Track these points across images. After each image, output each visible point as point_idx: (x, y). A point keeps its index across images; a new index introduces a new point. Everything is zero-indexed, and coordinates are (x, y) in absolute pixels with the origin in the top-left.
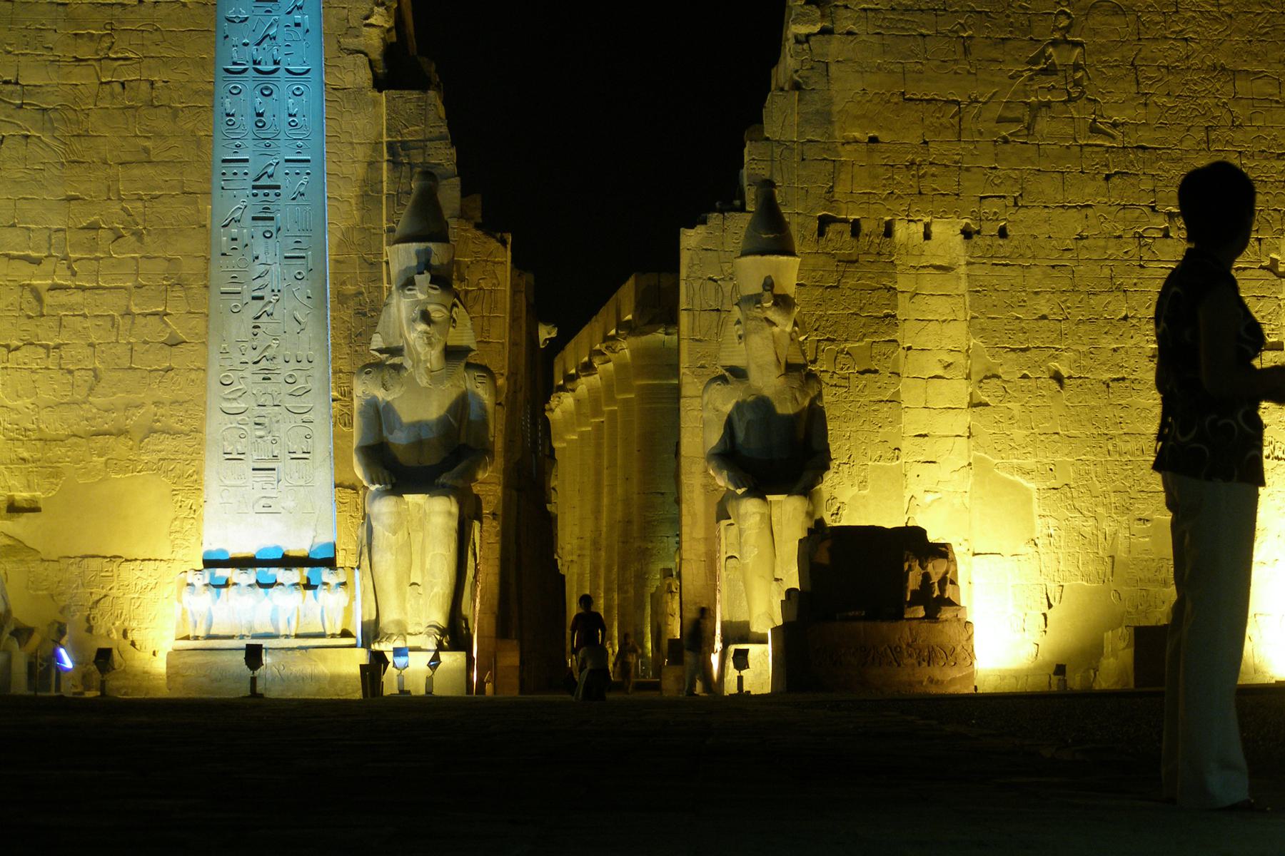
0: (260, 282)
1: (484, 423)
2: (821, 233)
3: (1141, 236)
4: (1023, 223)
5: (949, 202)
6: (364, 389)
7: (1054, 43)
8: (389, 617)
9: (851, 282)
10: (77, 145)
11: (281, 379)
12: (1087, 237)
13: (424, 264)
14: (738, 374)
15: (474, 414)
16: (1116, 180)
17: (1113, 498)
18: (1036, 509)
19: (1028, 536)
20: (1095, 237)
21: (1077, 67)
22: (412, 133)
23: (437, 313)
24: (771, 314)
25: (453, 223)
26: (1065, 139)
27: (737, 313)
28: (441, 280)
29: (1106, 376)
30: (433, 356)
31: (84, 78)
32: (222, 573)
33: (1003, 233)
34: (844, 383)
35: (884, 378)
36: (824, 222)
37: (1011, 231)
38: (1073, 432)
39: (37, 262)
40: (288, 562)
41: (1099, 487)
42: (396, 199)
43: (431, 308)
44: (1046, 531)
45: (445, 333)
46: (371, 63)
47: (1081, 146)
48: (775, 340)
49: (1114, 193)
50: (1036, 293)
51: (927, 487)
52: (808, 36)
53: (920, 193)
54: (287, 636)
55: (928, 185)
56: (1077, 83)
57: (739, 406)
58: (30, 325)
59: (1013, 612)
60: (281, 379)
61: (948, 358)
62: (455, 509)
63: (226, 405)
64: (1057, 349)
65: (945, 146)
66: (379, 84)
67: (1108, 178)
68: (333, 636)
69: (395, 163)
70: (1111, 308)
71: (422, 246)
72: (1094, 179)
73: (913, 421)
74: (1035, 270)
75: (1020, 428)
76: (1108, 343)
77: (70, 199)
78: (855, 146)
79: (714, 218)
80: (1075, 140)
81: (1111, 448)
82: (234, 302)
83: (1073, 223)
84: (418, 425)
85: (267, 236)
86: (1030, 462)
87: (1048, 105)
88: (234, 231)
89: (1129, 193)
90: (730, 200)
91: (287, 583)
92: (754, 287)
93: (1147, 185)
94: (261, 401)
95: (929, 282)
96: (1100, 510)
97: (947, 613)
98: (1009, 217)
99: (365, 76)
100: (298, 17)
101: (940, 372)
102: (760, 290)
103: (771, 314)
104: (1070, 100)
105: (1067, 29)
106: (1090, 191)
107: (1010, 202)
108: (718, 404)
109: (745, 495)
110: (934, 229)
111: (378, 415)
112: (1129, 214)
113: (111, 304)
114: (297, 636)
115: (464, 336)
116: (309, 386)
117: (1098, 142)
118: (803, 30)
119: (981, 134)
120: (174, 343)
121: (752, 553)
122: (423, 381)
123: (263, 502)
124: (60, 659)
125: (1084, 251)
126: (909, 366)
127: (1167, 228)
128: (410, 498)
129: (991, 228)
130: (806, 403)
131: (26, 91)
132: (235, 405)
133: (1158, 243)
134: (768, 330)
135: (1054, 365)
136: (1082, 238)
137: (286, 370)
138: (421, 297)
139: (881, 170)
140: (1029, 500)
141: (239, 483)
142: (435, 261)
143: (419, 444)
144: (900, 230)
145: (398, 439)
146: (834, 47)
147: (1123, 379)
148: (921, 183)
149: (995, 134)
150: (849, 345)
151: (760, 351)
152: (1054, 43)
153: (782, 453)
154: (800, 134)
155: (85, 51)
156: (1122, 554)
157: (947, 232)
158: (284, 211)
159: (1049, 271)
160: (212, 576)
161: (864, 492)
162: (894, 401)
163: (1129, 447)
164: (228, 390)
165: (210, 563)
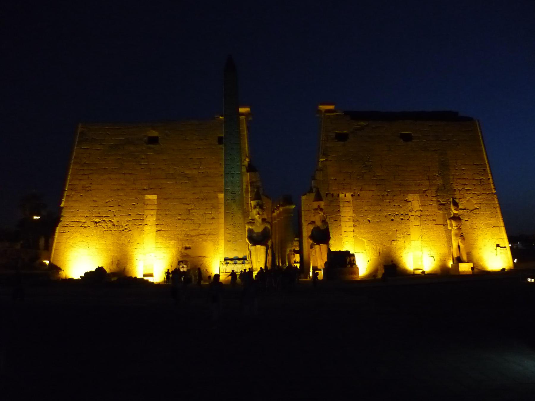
4: (363, 193)
5: (349, 190)
14: (313, 222)
17: (379, 242)
18: (366, 244)
21: (371, 165)
22: (254, 180)
23: (261, 213)
25: (262, 196)
27: (313, 211)
30: (260, 221)
31: (195, 172)
32: (227, 261)
33: (359, 195)
35: (338, 221)
36: (327, 194)
37: (361, 195)
39: (189, 204)
41: (377, 240)
42: (251, 192)
46: (246, 168)
48: (320, 217)
59: (364, 265)
66: (248, 171)
69: (250, 185)
73: (344, 229)
77: (194, 193)
79: (308, 194)
83: (371, 193)
84: (258, 233)
85: (234, 202)
86: (364, 236)
90: (311, 191)
92: (316, 207)
95: (346, 204)
97: (354, 266)
110: (347, 195)
111: (250, 231)
113: (202, 212)
120: (213, 218)
121: (318, 254)
122: (258, 225)
126: (342, 219)
131: (186, 174)
151: (317, 219)
153: (322, 236)
155: (196, 167)
156: (381, 252)
157: (349, 195)
162: (340, 225)
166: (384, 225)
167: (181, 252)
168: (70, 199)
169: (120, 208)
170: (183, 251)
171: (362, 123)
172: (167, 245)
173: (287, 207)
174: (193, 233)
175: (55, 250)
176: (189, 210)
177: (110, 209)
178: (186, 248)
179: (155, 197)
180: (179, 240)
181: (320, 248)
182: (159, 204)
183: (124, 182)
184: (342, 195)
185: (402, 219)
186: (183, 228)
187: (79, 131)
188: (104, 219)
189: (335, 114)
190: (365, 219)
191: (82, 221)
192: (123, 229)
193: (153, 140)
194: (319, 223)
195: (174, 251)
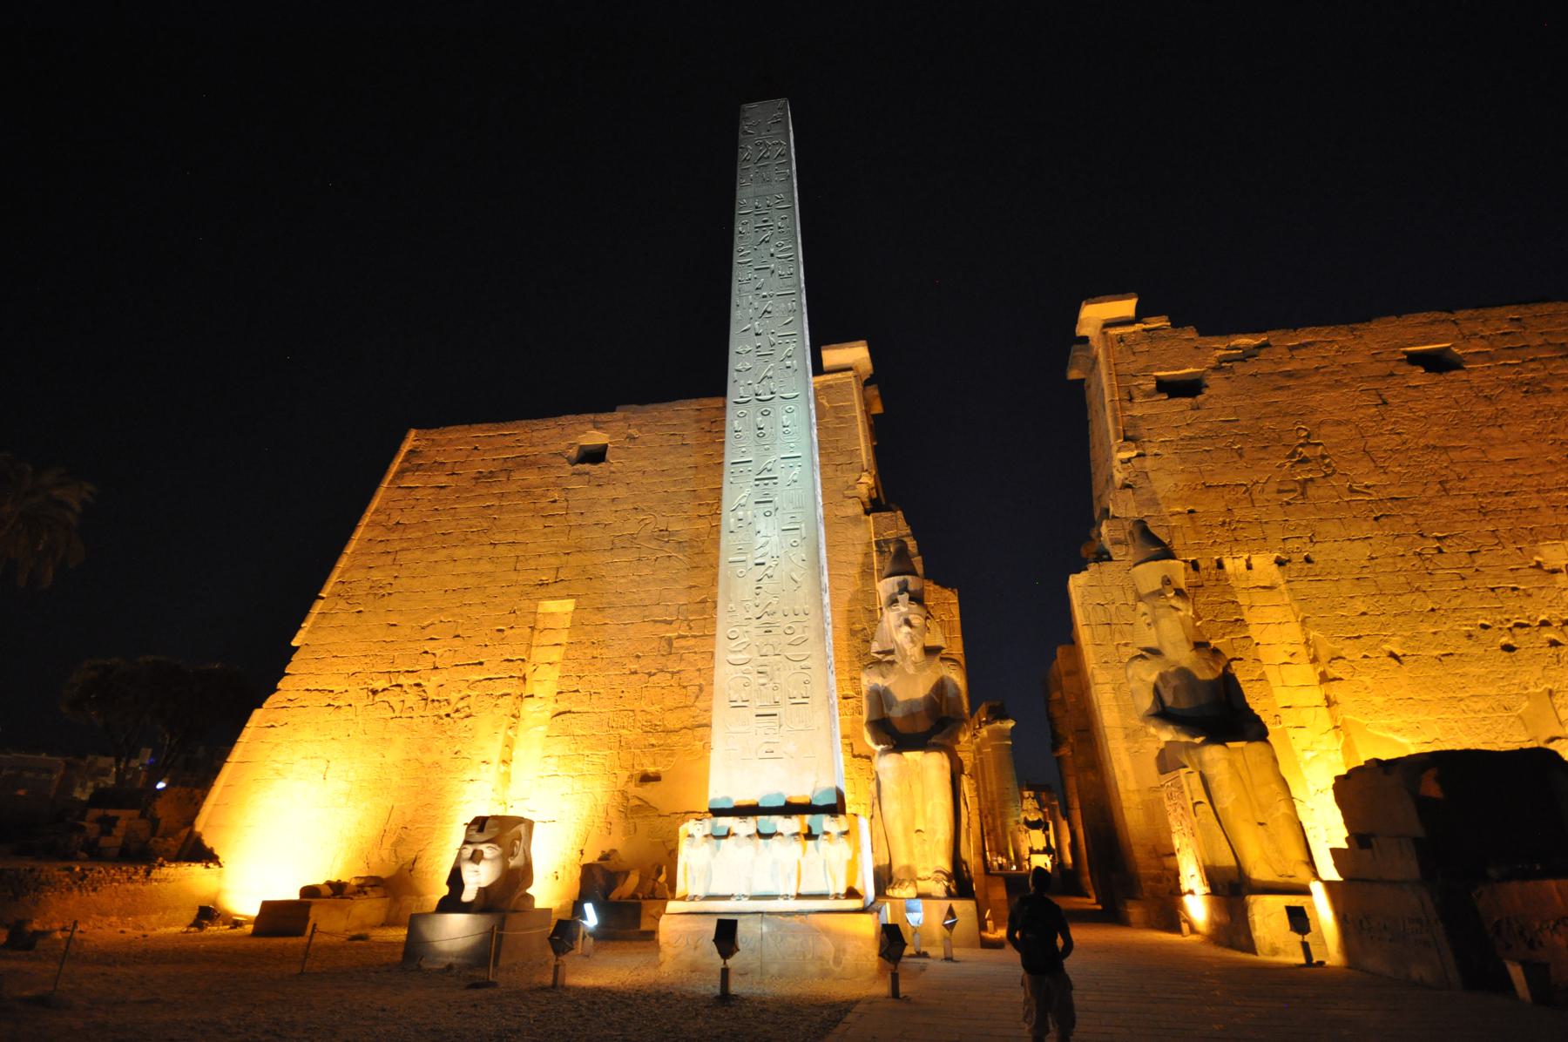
0: (762, 551)
1: (958, 697)
4: (1320, 553)
5: (1263, 543)
6: (869, 680)
7: (1301, 445)
8: (900, 861)
10: (697, 559)
11: (780, 631)
13: (903, 588)
14: (1155, 652)
15: (950, 693)
16: (1383, 520)
21: (1323, 457)
22: (890, 534)
24: (1174, 602)
28: (917, 598)
29: (1436, 653)
30: (915, 652)
33: (1308, 560)
37: (1312, 557)
39: (670, 623)
40: (789, 809)
43: (911, 617)
45: (923, 635)
52: (1129, 460)
54: (786, 897)
55: (1240, 535)
56: (1328, 466)
57: (1162, 676)
58: (663, 660)
60: (780, 631)
61: (1292, 650)
62: (947, 764)
63: (732, 657)
67: (1376, 519)
68: (837, 897)
69: (880, 552)
71: (901, 578)
76: (1427, 629)
82: (740, 568)
83: (1361, 551)
84: (911, 703)
86: (1396, 722)
87: (1311, 480)
88: (740, 514)
91: (787, 832)
93: (1410, 521)
94: (764, 651)
95: (1260, 598)
98: (1308, 550)
99: (859, 509)
100: (788, 363)
102: (1158, 586)
103: (1174, 602)
104: (1326, 476)
105: (1308, 437)
106: (1366, 528)
108: (1143, 675)
109: (1204, 743)
110: (1254, 562)
111: (880, 698)
114: (799, 896)
115: (936, 639)
116: (806, 635)
118: (1125, 455)
122: (911, 670)
123: (766, 747)
124: (584, 917)
128: (908, 755)
129: (1298, 558)
131: (671, 534)
132: (739, 656)
134: (1175, 614)
135: (1387, 647)
137: (786, 623)
138: (903, 609)
141: (743, 729)
142: (911, 588)
143: (911, 716)
144: (1229, 564)
145: (896, 713)
146: (1149, 463)
148: (1234, 533)
151: (1171, 632)
152: (1301, 445)
153: (1216, 711)
158: (780, 495)
160: (714, 826)
164: (734, 643)
165: (718, 812)
166: (1474, 670)
167: (623, 793)
168: (325, 623)
169: (458, 642)
170: (633, 789)
171: (1245, 341)
172: (579, 765)
173: (998, 724)
174: (672, 721)
175: (226, 786)
176: (670, 641)
177: (428, 646)
178: (646, 778)
179: (568, 605)
180: (622, 744)
181: (1231, 763)
182: (577, 624)
183: (489, 567)
186: (643, 704)
187: (406, 447)
188: (402, 680)
189: (1138, 327)
190: (1374, 648)
191: (337, 689)
192: (449, 710)
193: (595, 455)
194: (1184, 656)
195: (599, 791)
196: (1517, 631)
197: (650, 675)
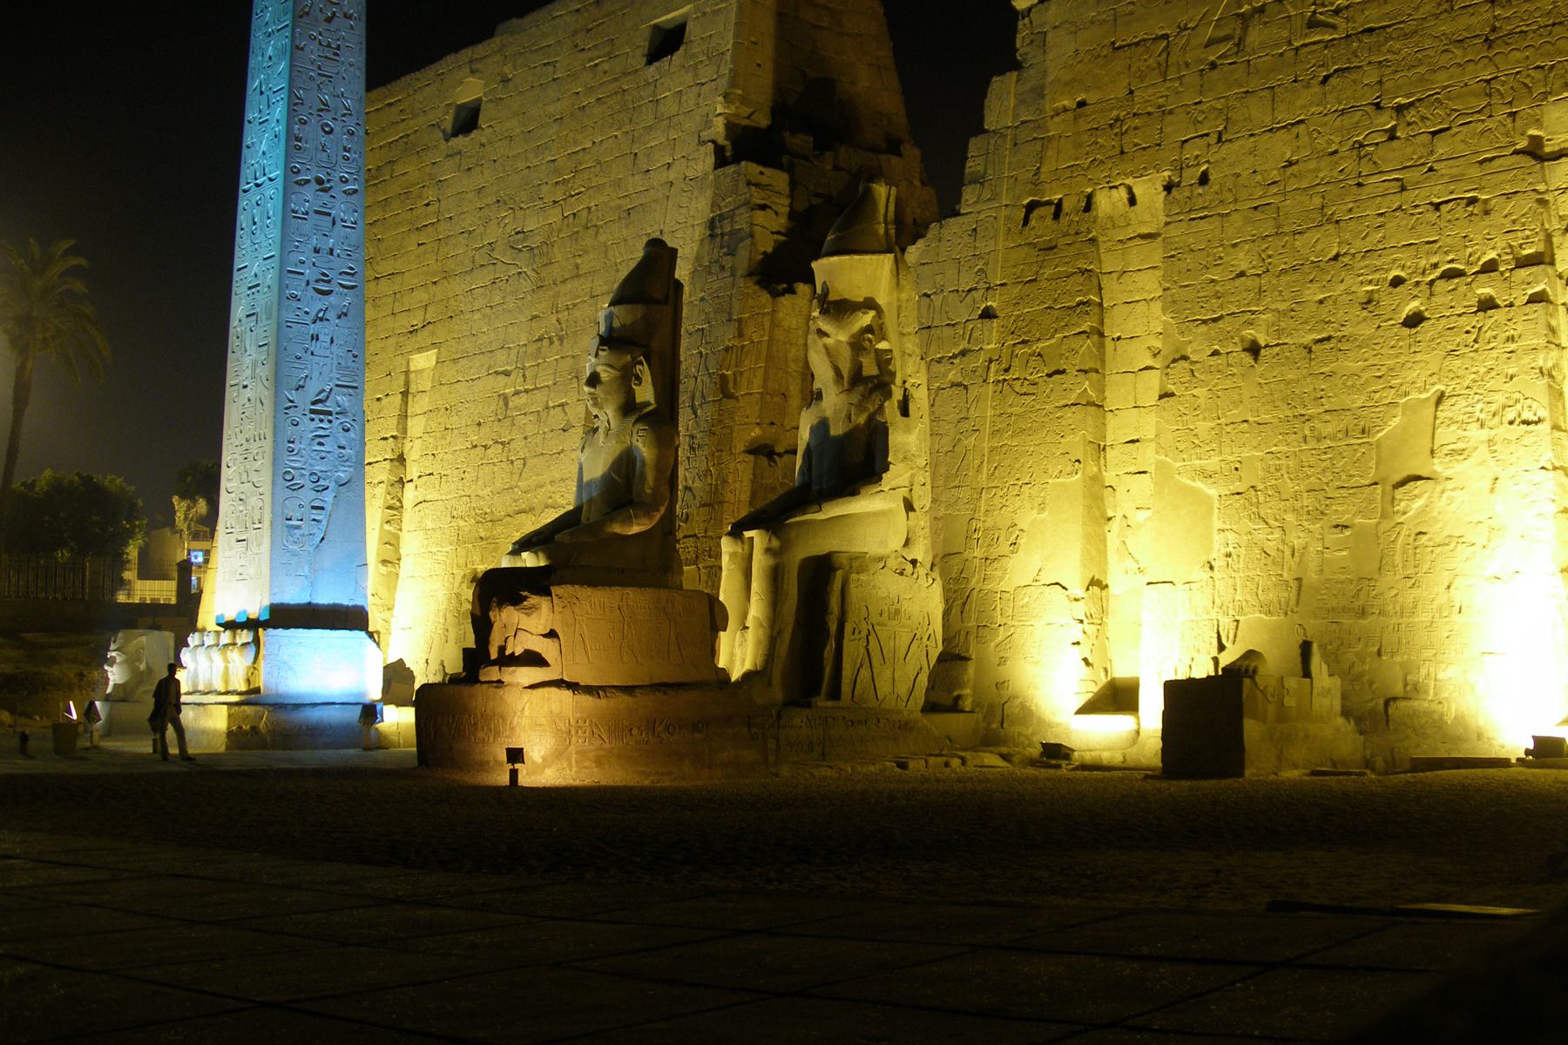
2: (1026, 221)
3: (1362, 146)
4: (1230, 161)
9: (1048, 272)
12: (1297, 162)
16: (1333, 81)
17: (1307, 501)
19: (1205, 558)
20: (1307, 159)
23: (605, 375)
26: (1278, 46)
29: (1309, 338)
31: (554, 216)
34: (1031, 389)
38: (1265, 417)
41: (1290, 487)
43: (599, 369)
44: (1224, 551)
47: (1297, 49)
49: (1330, 98)
50: (1235, 245)
51: (1140, 503)
53: (1122, 152)
64: (1253, 313)
65: (1150, 91)
70: (1319, 247)
72: (1308, 86)
74: (1235, 216)
75: (1205, 419)
78: (1063, 116)
80: (1290, 43)
81: (1307, 432)
83: (1282, 147)
86: (1213, 463)
89: (1349, 93)
96: (1290, 517)
101: (1150, 362)
106: (1304, 103)
107: (1213, 139)
112: (1347, 121)
117: (1317, 38)
119: (1187, 65)
125: (1292, 180)
127: (1394, 129)
129: (1192, 176)
130: (862, 420)
133: (1381, 150)
135: (1249, 333)
136: (1291, 164)
139: (1086, 137)
140: (1209, 513)
147: (1329, 338)
148: (1121, 141)
149: (1201, 61)
150: (1041, 345)
154: (1015, 117)
156: (1312, 576)
157: (1149, 190)
159: (1251, 214)
161: (1042, 516)
163: (1329, 429)
184: (1109, 202)
185: (1487, 305)
196: (1441, 286)
197: (485, 447)
